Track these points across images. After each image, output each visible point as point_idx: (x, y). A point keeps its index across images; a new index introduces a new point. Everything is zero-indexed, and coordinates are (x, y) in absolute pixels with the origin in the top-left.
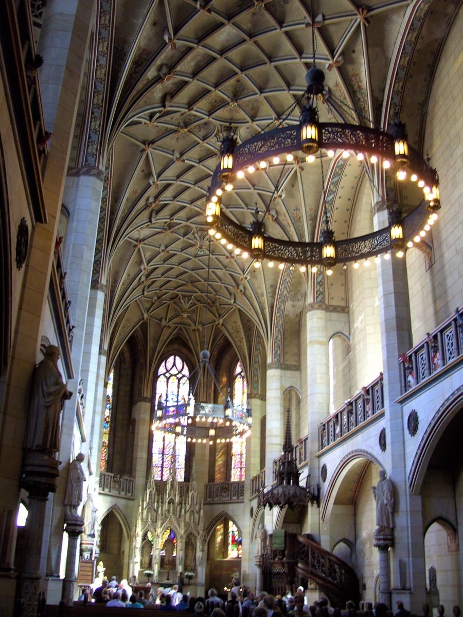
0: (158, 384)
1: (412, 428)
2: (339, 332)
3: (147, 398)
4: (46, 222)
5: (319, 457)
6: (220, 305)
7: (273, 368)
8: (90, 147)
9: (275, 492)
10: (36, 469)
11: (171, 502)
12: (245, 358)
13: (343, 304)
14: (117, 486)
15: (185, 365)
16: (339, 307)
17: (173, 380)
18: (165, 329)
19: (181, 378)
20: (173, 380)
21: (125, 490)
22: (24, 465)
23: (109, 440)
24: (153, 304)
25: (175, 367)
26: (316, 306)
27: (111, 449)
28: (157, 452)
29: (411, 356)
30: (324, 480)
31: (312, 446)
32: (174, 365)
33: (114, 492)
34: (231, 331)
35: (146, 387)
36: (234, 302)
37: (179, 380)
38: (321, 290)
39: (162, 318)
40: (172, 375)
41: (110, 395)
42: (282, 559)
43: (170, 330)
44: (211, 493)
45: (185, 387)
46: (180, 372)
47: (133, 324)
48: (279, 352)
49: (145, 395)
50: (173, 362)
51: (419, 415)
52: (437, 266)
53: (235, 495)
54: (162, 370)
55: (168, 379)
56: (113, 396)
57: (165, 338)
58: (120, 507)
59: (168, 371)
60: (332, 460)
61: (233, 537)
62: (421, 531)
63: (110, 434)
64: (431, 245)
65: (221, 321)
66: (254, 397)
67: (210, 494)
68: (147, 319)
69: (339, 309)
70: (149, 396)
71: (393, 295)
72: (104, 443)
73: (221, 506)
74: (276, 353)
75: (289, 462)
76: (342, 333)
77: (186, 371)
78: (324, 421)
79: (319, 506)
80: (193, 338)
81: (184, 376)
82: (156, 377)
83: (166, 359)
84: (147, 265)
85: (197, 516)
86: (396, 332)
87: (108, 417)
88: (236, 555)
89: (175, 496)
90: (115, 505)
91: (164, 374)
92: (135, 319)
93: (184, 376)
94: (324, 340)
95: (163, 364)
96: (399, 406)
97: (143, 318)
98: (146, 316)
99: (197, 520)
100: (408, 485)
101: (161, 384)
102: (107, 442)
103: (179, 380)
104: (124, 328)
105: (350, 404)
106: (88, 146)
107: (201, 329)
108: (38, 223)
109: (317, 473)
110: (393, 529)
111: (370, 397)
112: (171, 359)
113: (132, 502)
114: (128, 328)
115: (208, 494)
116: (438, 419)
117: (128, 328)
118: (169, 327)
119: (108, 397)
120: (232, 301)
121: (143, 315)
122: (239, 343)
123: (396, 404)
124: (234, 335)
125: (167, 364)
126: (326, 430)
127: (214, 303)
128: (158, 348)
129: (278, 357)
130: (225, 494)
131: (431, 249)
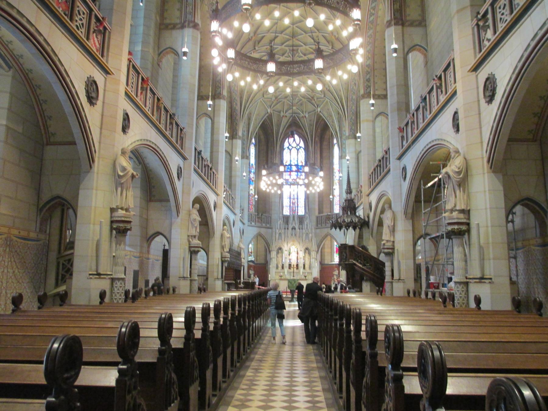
1: (403, 176)
2: (382, 112)
4: (113, 74)
5: (368, 195)
6: (317, 99)
7: (350, 138)
8: (188, 8)
9: (339, 220)
10: (117, 219)
13: (384, 93)
15: (301, 140)
16: (382, 95)
17: (294, 151)
20: (294, 151)
22: (111, 217)
24: (273, 102)
26: (366, 96)
29: (403, 129)
30: (371, 211)
31: (365, 190)
33: (258, 224)
36: (324, 96)
37: (298, 150)
38: (369, 84)
41: (254, 164)
42: (346, 261)
43: (288, 118)
45: (302, 153)
48: (353, 128)
51: (407, 168)
52: (429, 64)
54: (286, 144)
55: (290, 150)
57: (285, 124)
59: (290, 145)
60: (373, 198)
62: (411, 243)
64: (426, 48)
65: (319, 109)
68: (270, 112)
69: (377, 97)
71: (395, 87)
72: (251, 194)
74: (351, 129)
75: (349, 200)
76: (385, 113)
77: (302, 144)
78: (370, 173)
79: (368, 227)
80: (303, 121)
81: (300, 147)
82: (282, 149)
86: (397, 112)
89: (295, 224)
92: (263, 113)
93: (300, 147)
94: (371, 118)
95: (287, 140)
96: (398, 161)
97: (268, 112)
98: (269, 111)
100: (403, 213)
101: (286, 153)
103: (298, 150)
105: (380, 161)
106: (187, 7)
108: (109, 76)
109: (368, 207)
110: (394, 242)
111: (388, 157)
113: (270, 230)
116: (416, 171)
118: (286, 116)
120: (323, 96)
121: (267, 110)
123: (396, 160)
124: (328, 118)
126: (371, 179)
127: (313, 98)
128: (281, 131)
129: (353, 131)
131: (426, 50)
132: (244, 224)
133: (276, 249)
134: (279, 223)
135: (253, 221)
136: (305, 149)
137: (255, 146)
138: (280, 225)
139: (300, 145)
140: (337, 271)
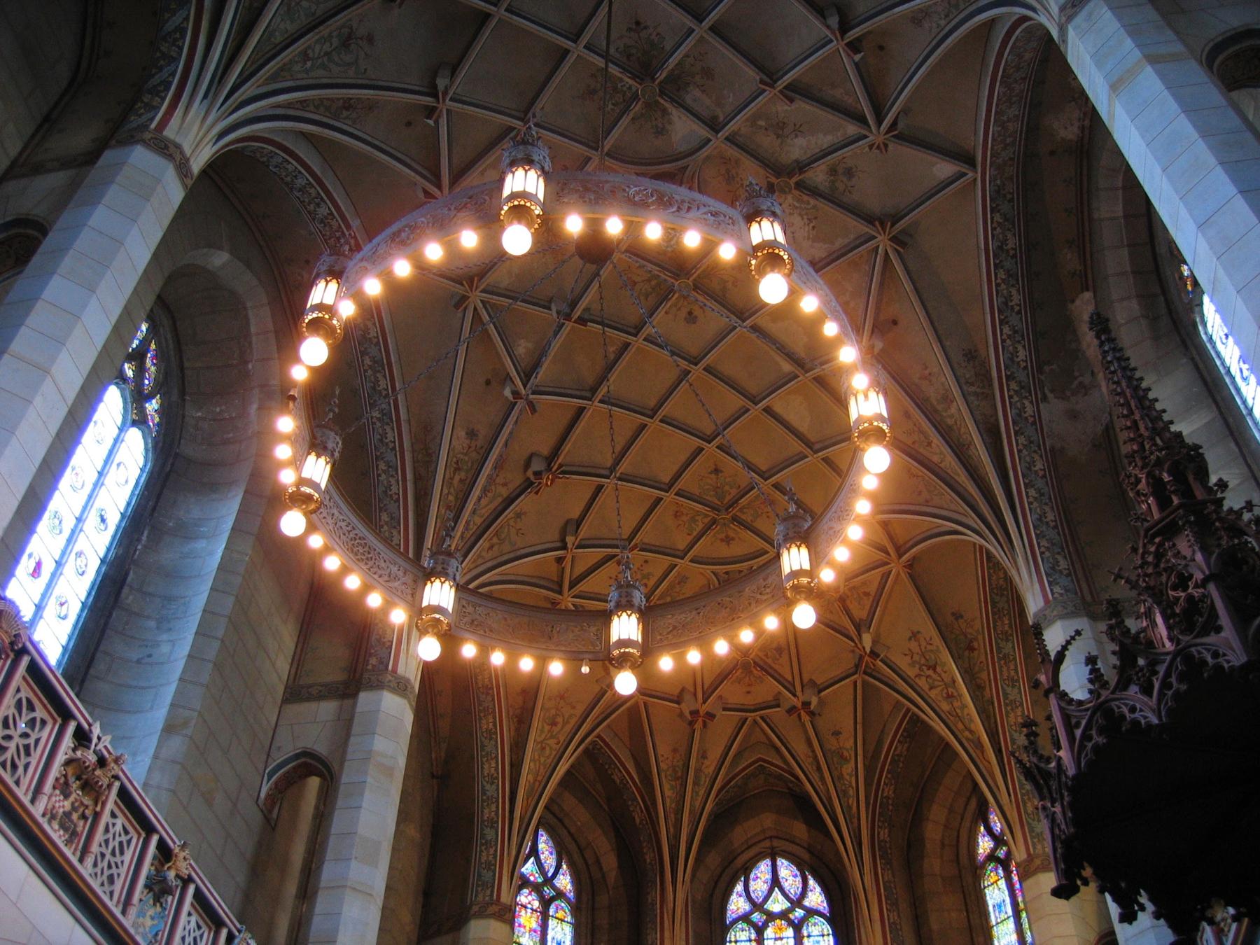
12: (979, 745)
15: (811, 882)
18: (698, 726)
19: (803, 921)
32: (775, 882)
34: (911, 672)
35: (667, 934)
37: (797, 927)
40: (771, 916)
46: (797, 902)
47: (580, 709)
50: (769, 876)
54: (737, 904)
55: (760, 930)
59: (757, 906)
65: (867, 641)
77: (816, 898)
83: (746, 871)
84: (525, 387)
91: (745, 918)
93: (811, 912)
95: (739, 887)
103: (797, 927)
104: (554, 724)
107: (815, 701)
112: (762, 871)
114: (565, 723)
117: (565, 723)
122: (945, 706)
124: (922, 683)
125: (754, 886)
129: (1064, 581)
136: (831, 920)
137: (576, 909)
139: (806, 903)
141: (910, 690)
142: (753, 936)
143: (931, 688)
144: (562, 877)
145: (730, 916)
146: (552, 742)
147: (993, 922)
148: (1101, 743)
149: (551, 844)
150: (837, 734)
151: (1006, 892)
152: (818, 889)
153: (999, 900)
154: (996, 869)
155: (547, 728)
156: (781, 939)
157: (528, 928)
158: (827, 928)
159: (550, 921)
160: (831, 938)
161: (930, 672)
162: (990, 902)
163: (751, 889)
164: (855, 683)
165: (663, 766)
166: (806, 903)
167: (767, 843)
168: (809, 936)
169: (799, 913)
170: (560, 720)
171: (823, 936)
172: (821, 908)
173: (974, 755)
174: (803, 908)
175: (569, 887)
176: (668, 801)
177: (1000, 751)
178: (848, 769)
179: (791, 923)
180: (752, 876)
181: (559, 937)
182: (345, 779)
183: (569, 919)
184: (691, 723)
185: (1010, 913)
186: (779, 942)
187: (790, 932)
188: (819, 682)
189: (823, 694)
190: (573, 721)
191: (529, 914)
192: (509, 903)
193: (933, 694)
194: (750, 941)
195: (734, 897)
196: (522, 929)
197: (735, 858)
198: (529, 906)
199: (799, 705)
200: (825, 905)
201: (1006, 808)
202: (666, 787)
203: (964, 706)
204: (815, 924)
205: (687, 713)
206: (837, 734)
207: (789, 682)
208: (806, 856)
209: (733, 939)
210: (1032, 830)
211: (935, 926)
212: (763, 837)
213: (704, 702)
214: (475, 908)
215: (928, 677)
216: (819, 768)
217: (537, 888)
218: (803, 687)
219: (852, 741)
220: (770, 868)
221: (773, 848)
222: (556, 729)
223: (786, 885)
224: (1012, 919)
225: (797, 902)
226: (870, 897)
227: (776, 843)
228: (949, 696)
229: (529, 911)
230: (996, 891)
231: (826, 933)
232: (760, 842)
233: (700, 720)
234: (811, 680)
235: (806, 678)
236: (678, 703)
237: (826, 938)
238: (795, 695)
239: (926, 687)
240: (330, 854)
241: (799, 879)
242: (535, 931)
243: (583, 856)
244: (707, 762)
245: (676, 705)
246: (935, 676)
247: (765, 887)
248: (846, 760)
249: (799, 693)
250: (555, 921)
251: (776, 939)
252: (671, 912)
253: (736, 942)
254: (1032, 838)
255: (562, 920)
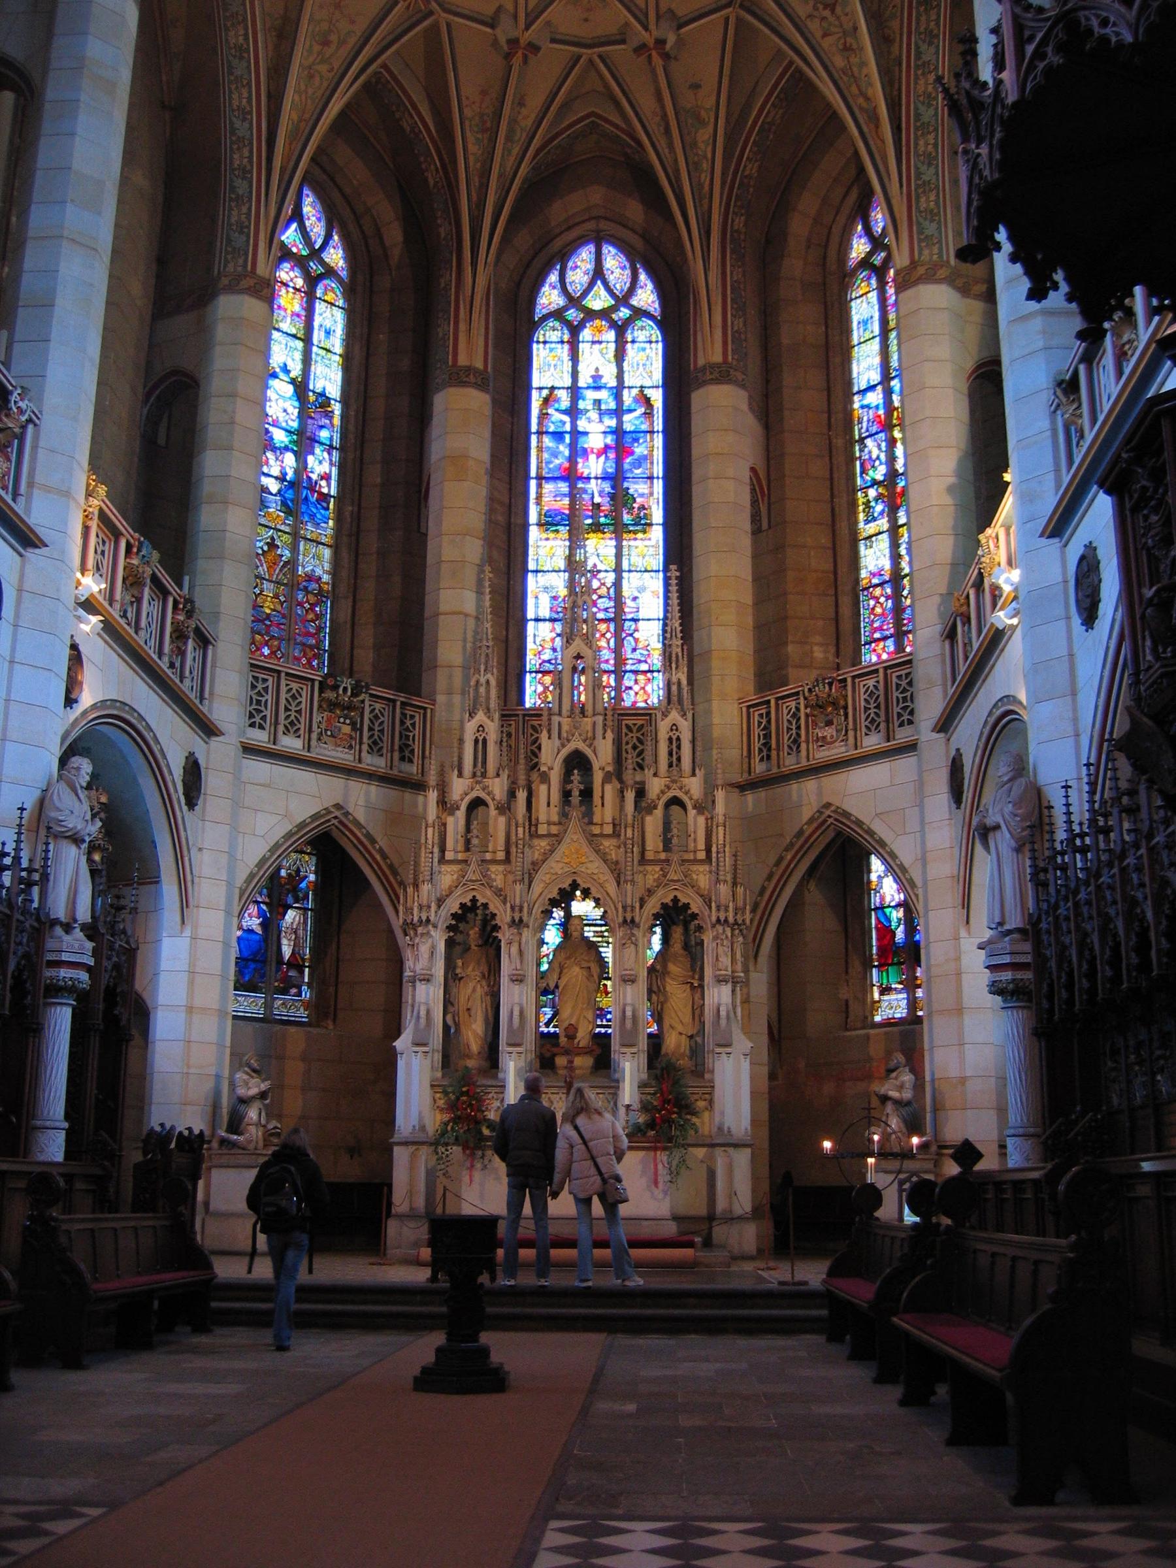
0: (539, 354)
3: (469, 369)
11: (577, 762)
12: (874, 118)
14: (347, 729)
15: (643, 277)
18: (517, 60)
19: (628, 322)
21: (386, 744)
23: (335, 572)
25: (599, 286)
27: (346, 606)
28: (545, 613)
32: (598, 274)
35: (462, 327)
37: (621, 330)
39: (499, 9)
40: (591, 315)
44: (767, 736)
46: (623, 300)
47: (362, 24)
49: (463, 360)
50: (590, 267)
53: (873, 725)
54: (550, 297)
56: (345, 400)
58: (360, 815)
59: (574, 301)
61: (886, 932)
63: (336, 548)
66: (930, 277)
67: (767, 745)
70: (479, 365)
73: (810, 785)
77: (646, 297)
83: (563, 257)
85: (697, 823)
87: (326, 477)
88: (901, 1012)
89: (591, 741)
90: (338, 806)
91: (558, 314)
93: (639, 313)
95: (553, 278)
99: (701, 845)
102: (326, 578)
103: (621, 330)
104: (326, 43)
107: (671, 39)
112: (584, 258)
115: (757, 746)
119: (324, 401)
122: (839, 61)
124: (814, 26)
125: (571, 276)
130: (829, 732)
132: (208, 729)
133: (442, 916)
134: (470, 727)
135: (291, 728)
136: (662, 324)
137: (350, 291)
138: (481, 745)
139: (634, 302)
140: (907, 1078)
141: (798, 35)
142: (566, 338)
143: (825, 35)
144: (332, 251)
145: (539, 312)
146: (323, 68)
147: (855, 342)
148: (1055, 63)
149: (319, 206)
150: (696, 87)
151: (876, 307)
152: (650, 286)
153: (866, 316)
154: (869, 278)
155: (317, 48)
156: (600, 342)
157: (289, 312)
158: (656, 334)
159: (317, 305)
160: (660, 345)
161: (827, 13)
162: (855, 318)
163: (567, 280)
164: (727, 19)
165: (468, 112)
166: (634, 302)
167: (591, 225)
168: (633, 342)
169: (624, 313)
170: (333, 38)
171: (651, 342)
172: (651, 309)
173: (865, 129)
174: (631, 307)
175: (341, 263)
176: (471, 159)
177: (899, 128)
178: (704, 135)
179: (613, 325)
180: (570, 264)
181: (328, 324)
182: (50, 94)
183: (341, 303)
184: (508, 56)
185: (877, 331)
186: (597, 346)
187: (611, 335)
188: (680, 13)
189: (683, 30)
190: (352, 41)
191: (290, 295)
192: (267, 276)
193: (826, 43)
194: (562, 342)
195: (546, 289)
196: (282, 313)
197: (552, 240)
198: (291, 284)
199: (651, 43)
200: (657, 305)
201: (894, 202)
202: (471, 138)
203: (863, 64)
204: (642, 328)
205: (502, 40)
206: (696, 87)
207: (641, 10)
208: (638, 243)
209: (541, 339)
210: (920, 232)
211: (785, 341)
212: (586, 217)
213: (527, 28)
214: (225, 281)
215: (824, 19)
216: (667, 131)
217: (300, 262)
218: (658, 17)
219: (714, 98)
220: (593, 256)
221: (598, 232)
222: (329, 51)
223: (611, 279)
224: (878, 339)
225: (623, 300)
226: (713, 299)
227: (603, 225)
228: (847, 49)
229: (291, 290)
230: (865, 305)
231: (654, 339)
232: (583, 222)
233: (520, 54)
234: (670, 11)
235: (663, 8)
236: (492, 27)
237: (653, 345)
238: (646, 28)
239: (818, 34)
240: (36, 196)
241: (628, 272)
242: (298, 315)
243: (360, 227)
244: (524, 111)
245: (488, 30)
246: (831, 19)
247: (586, 279)
248: (703, 123)
249: (652, 26)
250: (324, 305)
251: (593, 342)
252: (468, 303)
253: (545, 342)
254: (920, 241)
255: (332, 304)
